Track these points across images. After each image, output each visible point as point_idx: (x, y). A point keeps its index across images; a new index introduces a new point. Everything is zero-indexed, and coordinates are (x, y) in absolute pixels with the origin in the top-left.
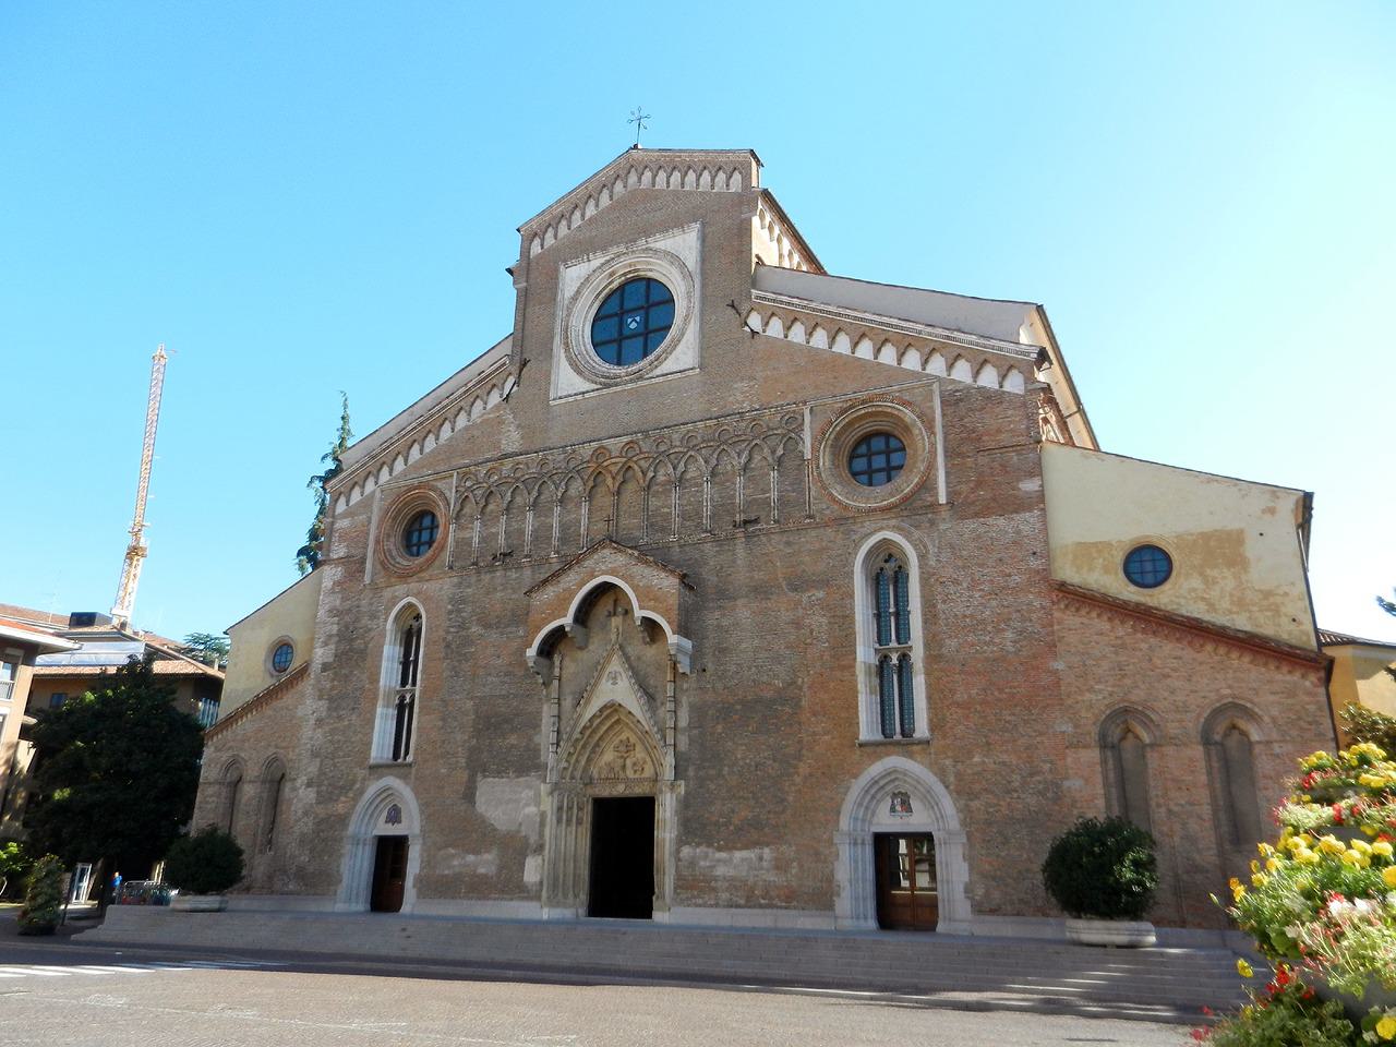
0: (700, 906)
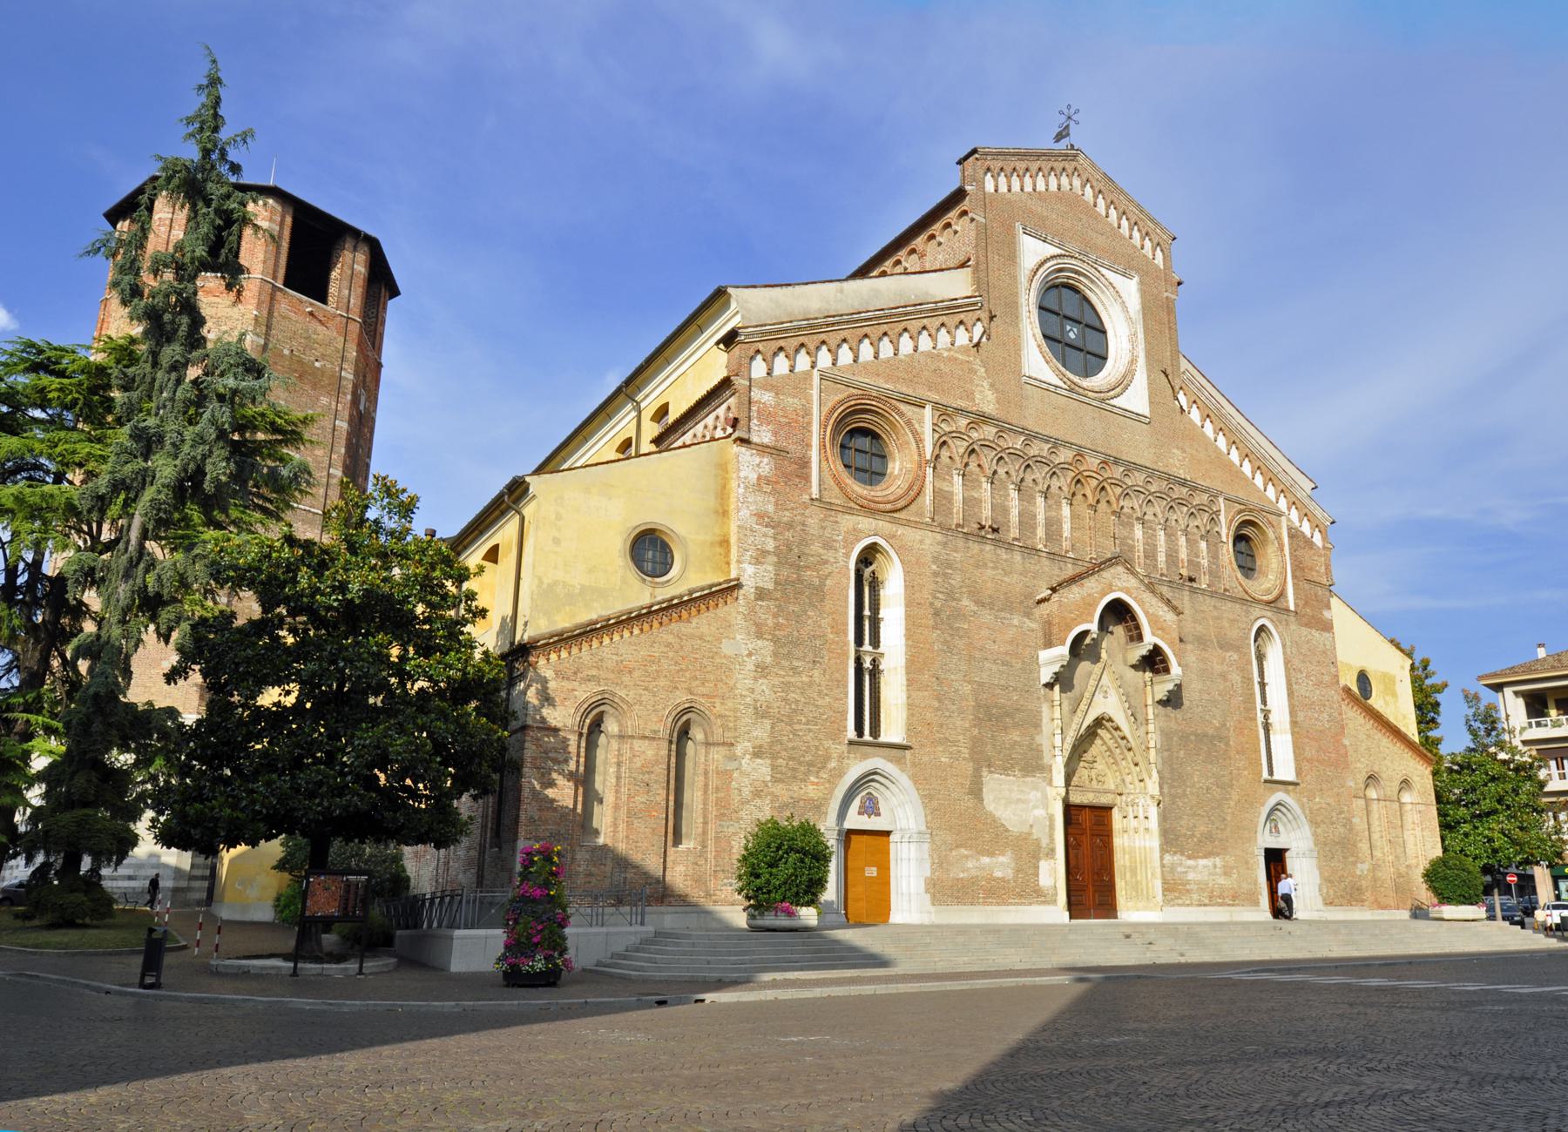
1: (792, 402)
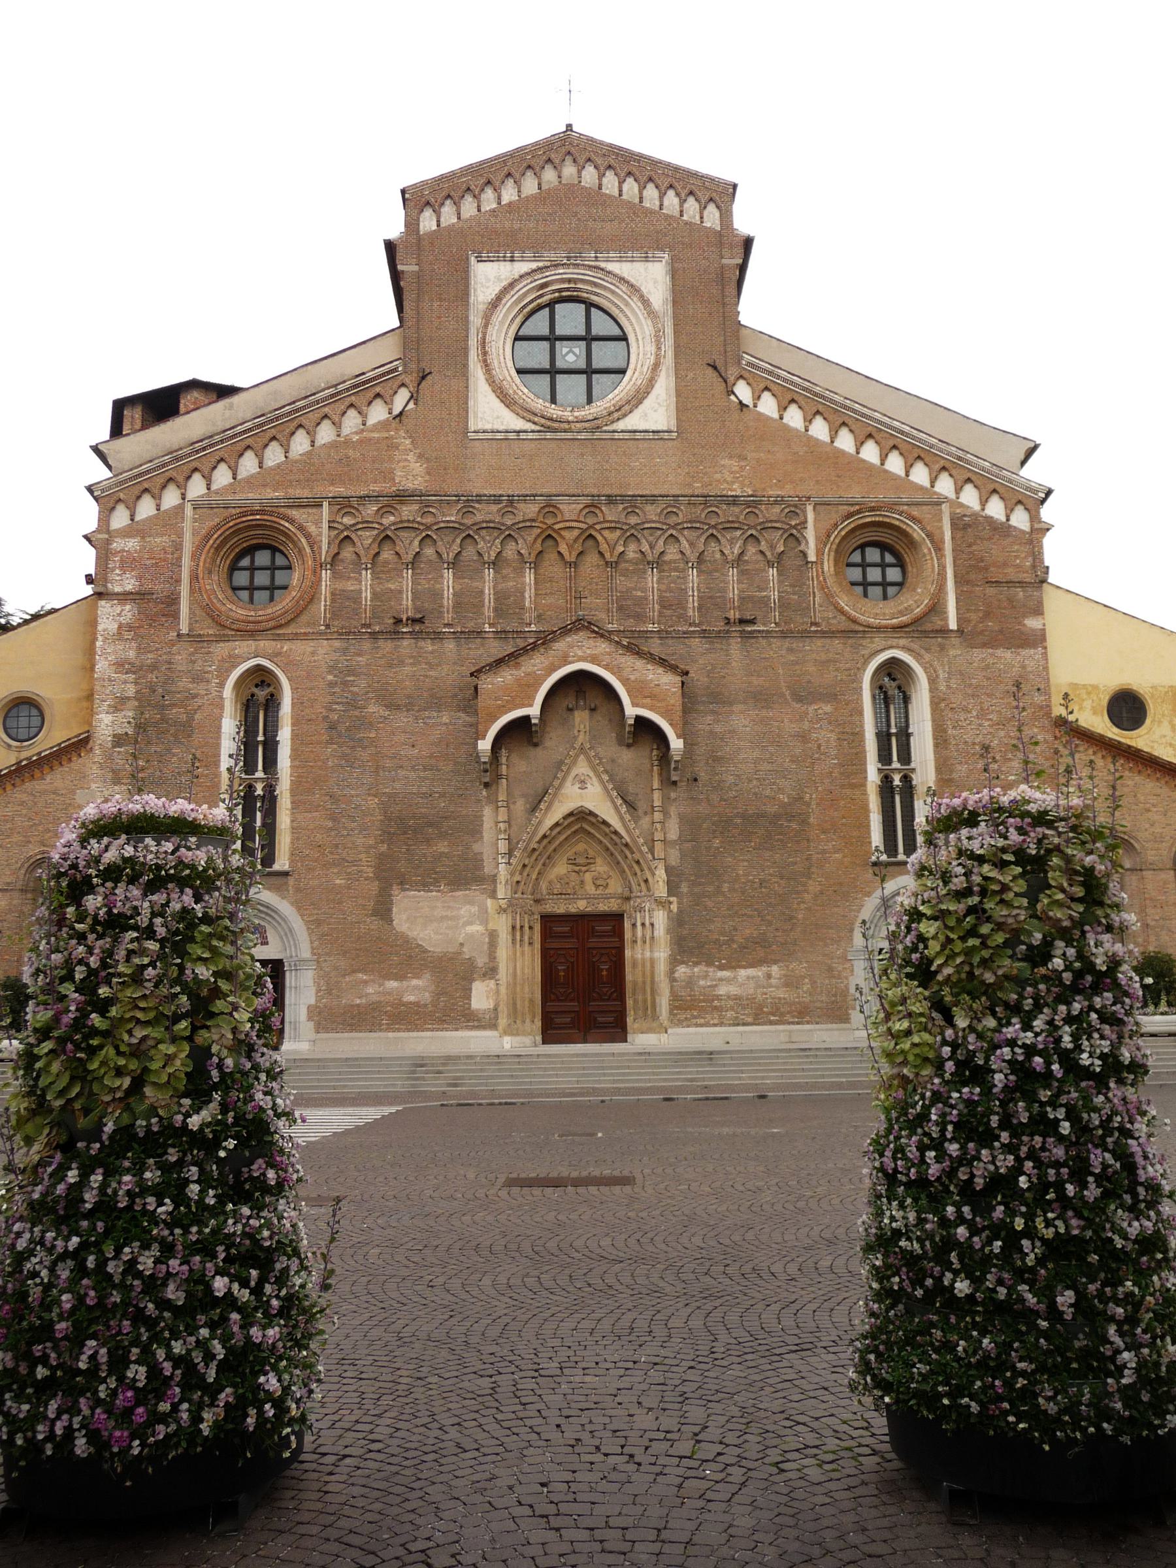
0: (701, 1025)
1: (160, 541)
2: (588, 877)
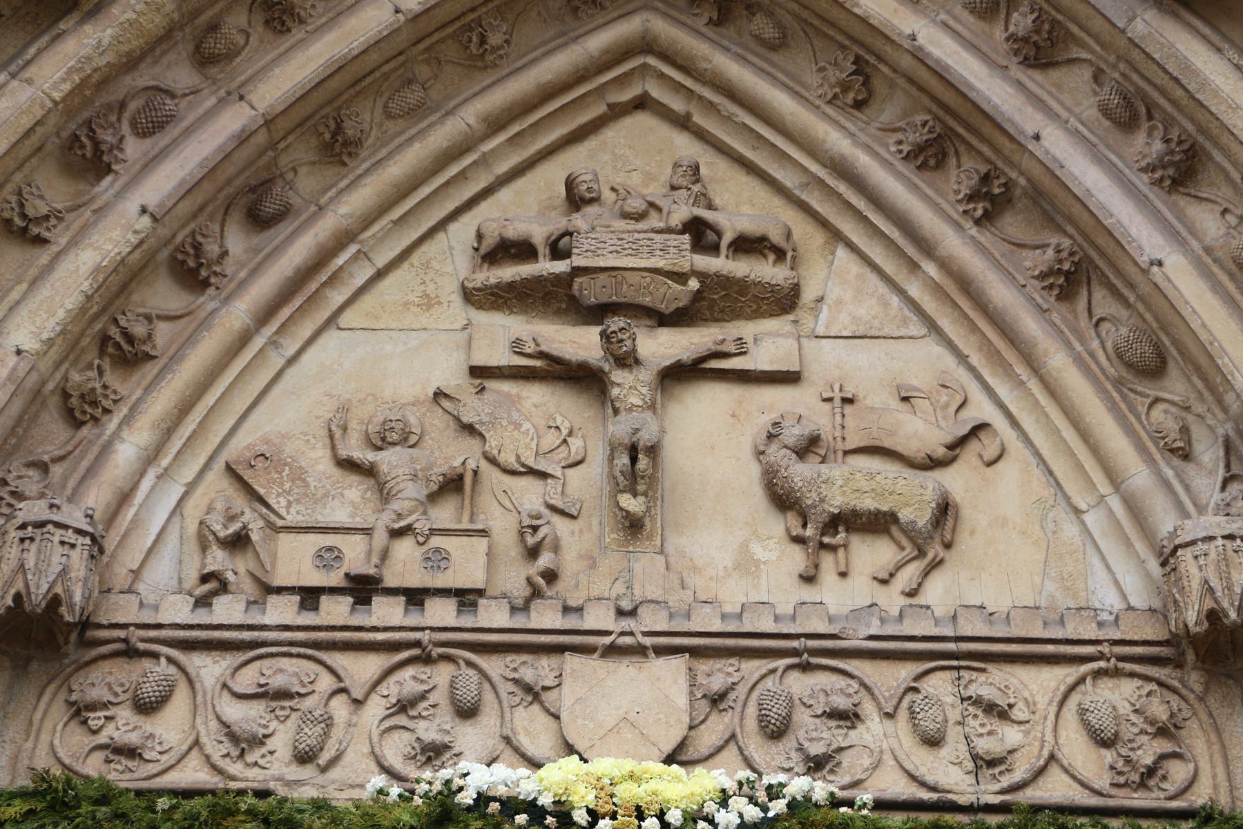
2: (711, 437)
